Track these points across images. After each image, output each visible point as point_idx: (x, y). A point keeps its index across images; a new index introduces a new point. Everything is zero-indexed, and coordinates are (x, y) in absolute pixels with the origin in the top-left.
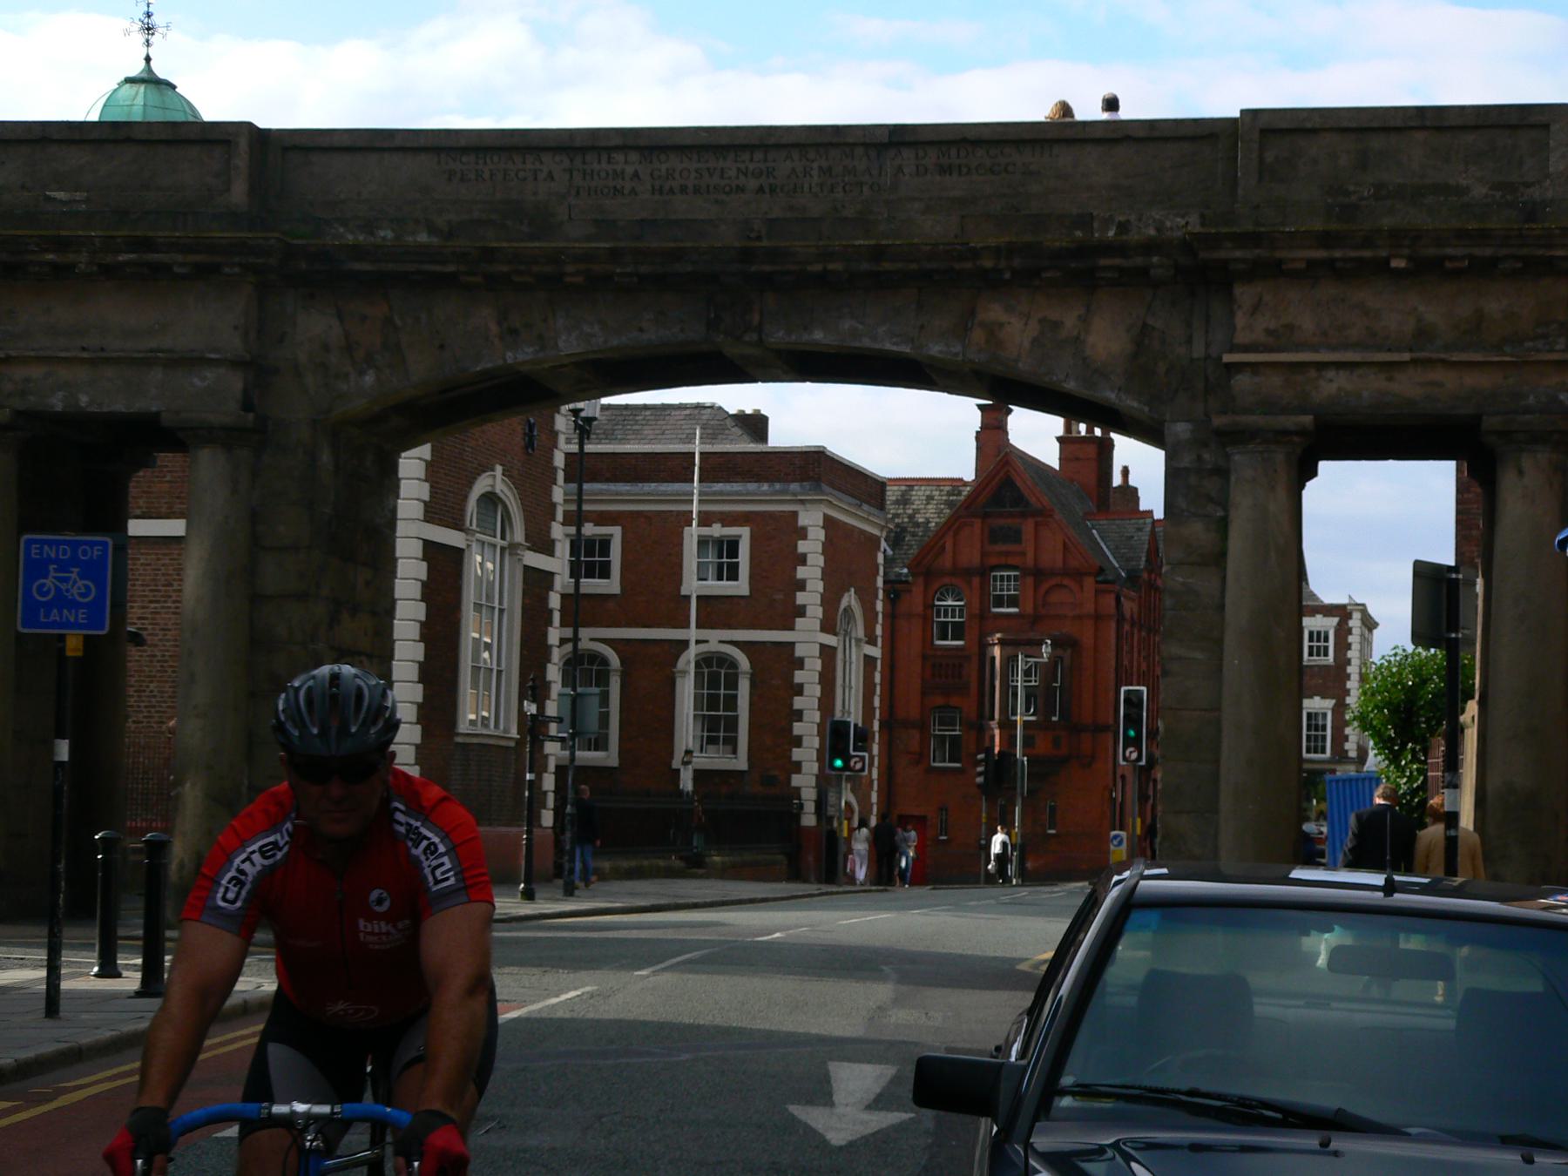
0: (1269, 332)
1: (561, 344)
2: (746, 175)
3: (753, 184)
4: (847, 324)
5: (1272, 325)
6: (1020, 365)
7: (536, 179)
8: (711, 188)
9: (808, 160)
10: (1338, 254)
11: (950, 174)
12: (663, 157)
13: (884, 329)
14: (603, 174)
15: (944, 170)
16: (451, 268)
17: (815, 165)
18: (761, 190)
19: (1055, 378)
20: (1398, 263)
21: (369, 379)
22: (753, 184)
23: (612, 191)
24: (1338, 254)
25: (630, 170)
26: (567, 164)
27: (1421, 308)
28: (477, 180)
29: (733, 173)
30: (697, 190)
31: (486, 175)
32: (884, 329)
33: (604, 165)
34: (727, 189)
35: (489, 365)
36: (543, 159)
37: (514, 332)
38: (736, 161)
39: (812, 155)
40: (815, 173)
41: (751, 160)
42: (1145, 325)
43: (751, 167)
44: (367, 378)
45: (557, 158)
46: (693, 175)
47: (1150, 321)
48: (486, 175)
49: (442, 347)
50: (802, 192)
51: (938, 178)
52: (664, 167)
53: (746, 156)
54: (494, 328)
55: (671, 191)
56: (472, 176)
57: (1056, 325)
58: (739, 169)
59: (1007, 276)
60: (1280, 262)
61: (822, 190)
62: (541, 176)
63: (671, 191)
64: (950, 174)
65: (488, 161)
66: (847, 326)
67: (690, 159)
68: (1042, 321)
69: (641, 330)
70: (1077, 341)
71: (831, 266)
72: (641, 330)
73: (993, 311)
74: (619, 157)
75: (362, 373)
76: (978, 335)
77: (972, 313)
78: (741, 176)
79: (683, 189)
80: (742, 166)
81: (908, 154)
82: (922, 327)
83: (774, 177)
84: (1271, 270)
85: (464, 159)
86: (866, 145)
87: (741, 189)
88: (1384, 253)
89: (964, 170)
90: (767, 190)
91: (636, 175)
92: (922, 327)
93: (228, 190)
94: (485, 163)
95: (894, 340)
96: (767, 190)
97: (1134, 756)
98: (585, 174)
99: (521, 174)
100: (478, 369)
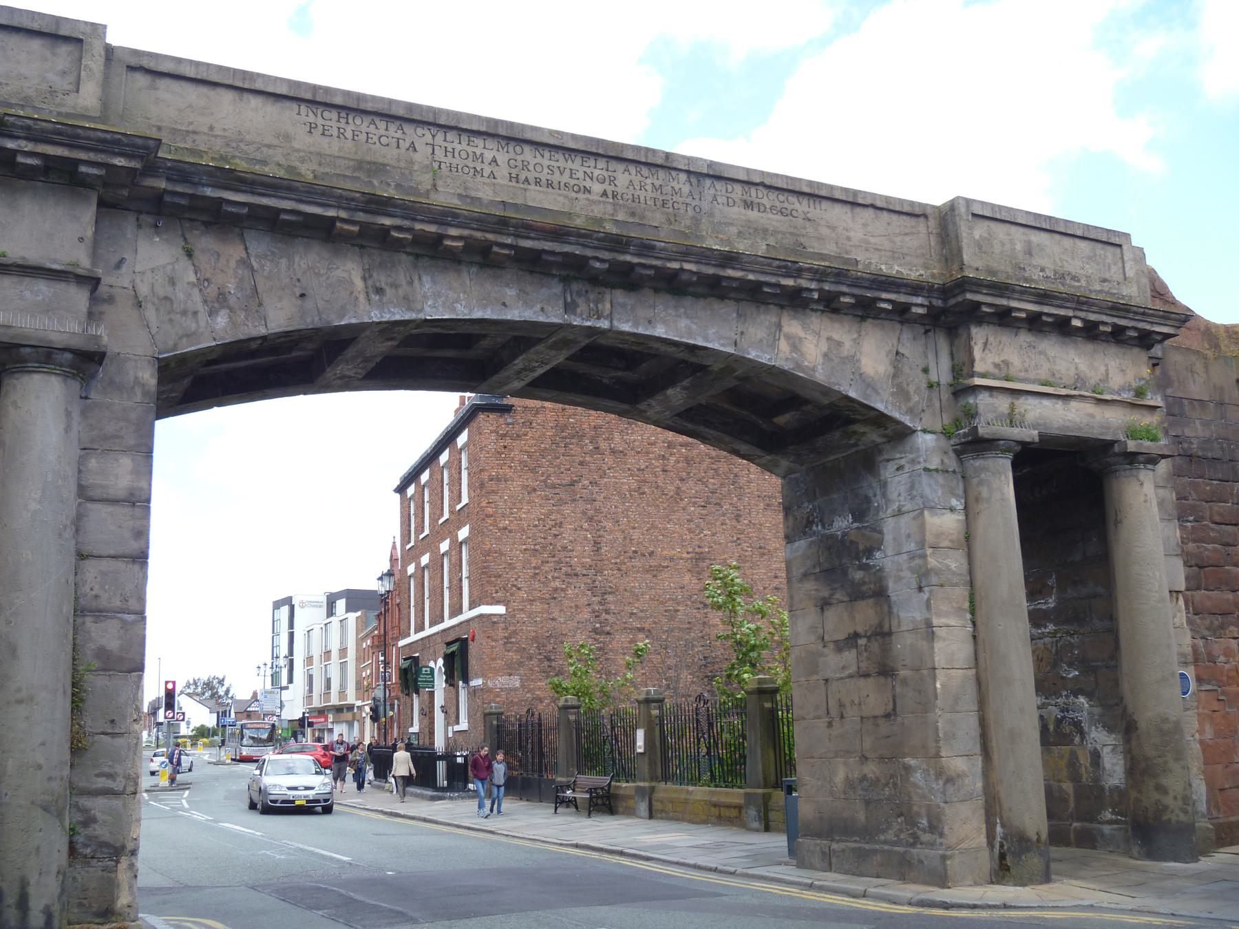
0: (997, 366)
1: (427, 309)
2: (592, 179)
3: (597, 188)
4: (683, 323)
5: (997, 360)
6: (817, 374)
7: (398, 147)
8: (562, 184)
9: (642, 176)
10: (1046, 309)
11: (752, 210)
12: (518, 149)
13: (713, 331)
14: (464, 155)
15: (748, 205)
16: (331, 213)
17: (649, 181)
18: (605, 194)
19: (842, 389)
20: (1077, 323)
21: (222, 320)
22: (597, 188)
23: (472, 170)
24: (1046, 309)
25: (488, 156)
26: (428, 138)
27: (1077, 360)
28: (339, 137)
29: (580, 175)
30: (550, 184)
31: (349, 134)
32: (713, 331)
33: (464, 145)
34: (576, 188)
35: (354, 321)
36: (405, 130)
37: (379, 291)
38: (582, 165)
39: (645, 171)
40: (649, 187)
41: (595, 168)
42: (897, 353)
43: (596, 172)
44: (219, 319)
45: (420, 131)
46: (546, 170)
47: (901, 351)
48: (349, 134)
49: (302, 295)
50: (639, 202)
51: (743, 210)
52: (519, 158)
53: (592, 162)
54: (359, 284)
55: (527, 180)
56: (335, 133)
57: (839, 344)
58: (585, 172)
59: (816, 296)
60: (1010, 310)
61: (655, 205)
62: (405, 145)
63: (527, 180)
64: (752, 210)
65: (350, 121)
66: (683, 325)
67: (543, 156)
68: (829, 339)
69: (504, 304)
70: (852, 360)
71: (687, 266)
72: (504, 304)
73: (792, 326)
74: (479, 142)
75: (212, 313)
76: (783, 345)
77: (779, 326)
78: (587, 178)
79: (538, 182)
80: (588, 171)
81: (719, 185)
82: (742, 333)
83: (615, 185)
84: (1003, 318)
85: (326, 114)
86: (688, 172)
87: (587, 190)
88: (1070, 313)
89: (762, 208)
90: (610, 195)
91: (494, 161)
92: (742, 333)
93: (78, 91)
94: (347, 123)
95: (722, 341)
96: (610, 195)
97: (171, 715)
98: (446, 151)
99: (384, 140)
100: (343, 323)
